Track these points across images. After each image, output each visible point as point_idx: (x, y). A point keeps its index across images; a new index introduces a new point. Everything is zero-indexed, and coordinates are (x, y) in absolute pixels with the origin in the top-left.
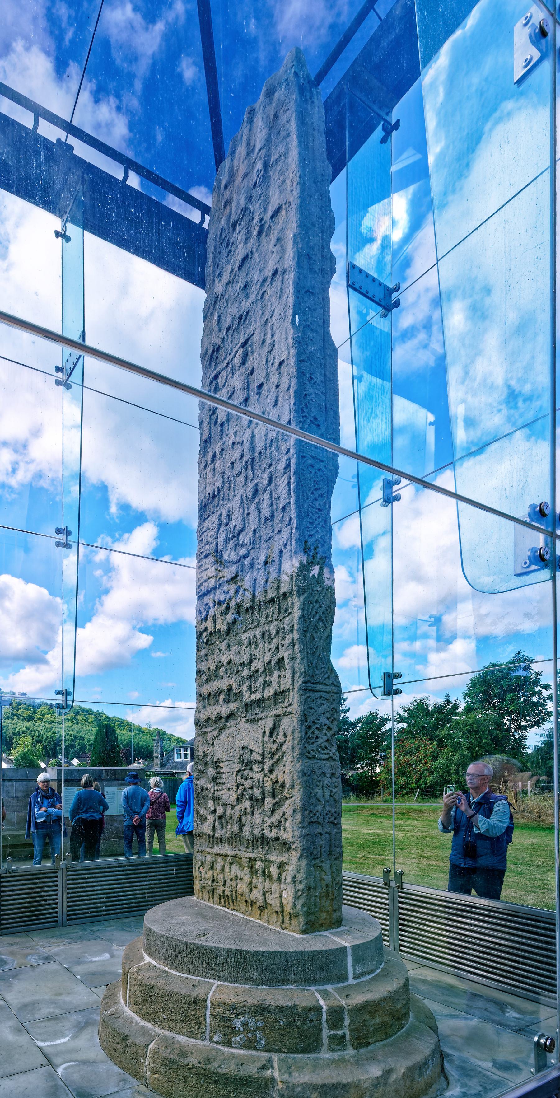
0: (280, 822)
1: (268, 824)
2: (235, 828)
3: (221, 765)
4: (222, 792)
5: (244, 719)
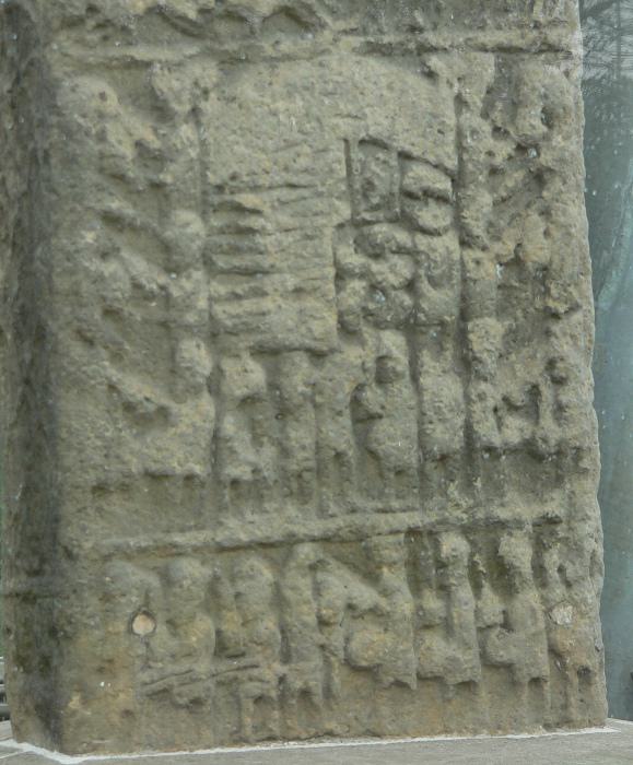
0: (534, 391)
1: (491, 403)
2: (340, 434)
3: (248, 200)
4: (267, 304)
5: (357, 41)
